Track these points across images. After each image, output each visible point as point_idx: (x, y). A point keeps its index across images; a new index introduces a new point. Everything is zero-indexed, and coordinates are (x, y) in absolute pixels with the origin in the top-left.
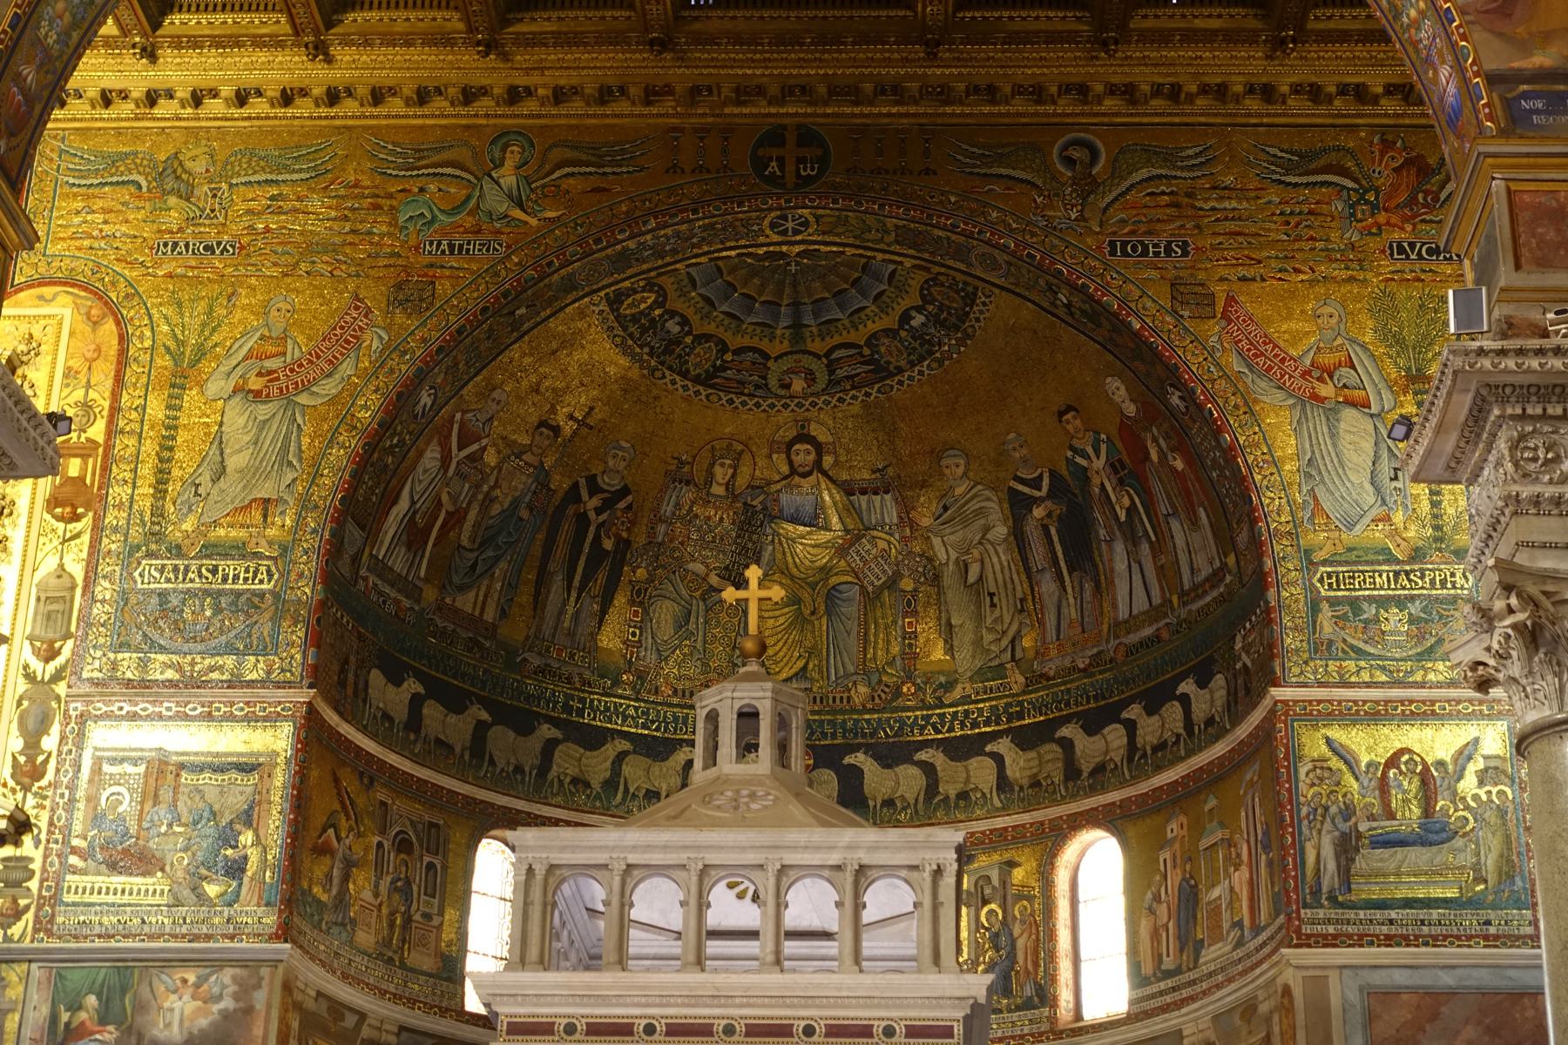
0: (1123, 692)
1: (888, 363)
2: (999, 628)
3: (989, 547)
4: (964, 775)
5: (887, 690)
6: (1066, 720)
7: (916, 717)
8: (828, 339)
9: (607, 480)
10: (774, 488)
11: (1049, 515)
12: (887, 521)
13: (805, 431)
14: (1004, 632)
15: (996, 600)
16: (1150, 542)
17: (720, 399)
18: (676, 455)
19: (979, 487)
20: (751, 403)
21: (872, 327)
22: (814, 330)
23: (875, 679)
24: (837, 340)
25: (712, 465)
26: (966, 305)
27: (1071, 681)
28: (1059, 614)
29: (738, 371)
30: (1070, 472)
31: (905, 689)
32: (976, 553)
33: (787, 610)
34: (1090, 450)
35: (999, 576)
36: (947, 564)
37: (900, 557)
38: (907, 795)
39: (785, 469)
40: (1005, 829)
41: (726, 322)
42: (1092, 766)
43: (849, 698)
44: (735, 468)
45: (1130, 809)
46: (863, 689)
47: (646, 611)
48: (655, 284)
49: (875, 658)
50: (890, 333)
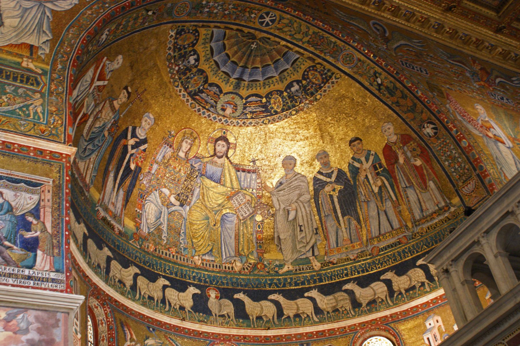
0: (379, 268)
1: (272, 108)
2: (304, 241)
3: (301, 204)
4: (296, 306)
5: (250, 266)
7: (266, 280)
8: (250, 90)
9: (140, 132)
10: (206, 160)
11: (334, 190)
12: (252, 187)
13: (225, 135)
14: (307, 243)
15: (303, 228)
17: (195, 108)
18: (169, 130)
19: (299, 176)
20: (207, 114)
21: (272, 88)
22: (246, 83)
23: (244, 260)
24: (254, 91)
25: (182, 141)
26: (323, 82)
27: (347, 265)
28: (337, 235)
29: (208, 95)
30: (349, 170)
31: (259, 266)
33: (203, 222)
34: (363, 159)
35: (305, 218)
36: (279, 210)
38: (268, 315)
39: (212, 153)
40: (324, 331)
41: (213, 67)
42: (367, 301)
43: (232, 268)
44: (191, 145)
45: (398, 318)
46: (239, 264)
47: (144, 205)
48: (197, 31)
49: (243, 250)
50: (280, 93)
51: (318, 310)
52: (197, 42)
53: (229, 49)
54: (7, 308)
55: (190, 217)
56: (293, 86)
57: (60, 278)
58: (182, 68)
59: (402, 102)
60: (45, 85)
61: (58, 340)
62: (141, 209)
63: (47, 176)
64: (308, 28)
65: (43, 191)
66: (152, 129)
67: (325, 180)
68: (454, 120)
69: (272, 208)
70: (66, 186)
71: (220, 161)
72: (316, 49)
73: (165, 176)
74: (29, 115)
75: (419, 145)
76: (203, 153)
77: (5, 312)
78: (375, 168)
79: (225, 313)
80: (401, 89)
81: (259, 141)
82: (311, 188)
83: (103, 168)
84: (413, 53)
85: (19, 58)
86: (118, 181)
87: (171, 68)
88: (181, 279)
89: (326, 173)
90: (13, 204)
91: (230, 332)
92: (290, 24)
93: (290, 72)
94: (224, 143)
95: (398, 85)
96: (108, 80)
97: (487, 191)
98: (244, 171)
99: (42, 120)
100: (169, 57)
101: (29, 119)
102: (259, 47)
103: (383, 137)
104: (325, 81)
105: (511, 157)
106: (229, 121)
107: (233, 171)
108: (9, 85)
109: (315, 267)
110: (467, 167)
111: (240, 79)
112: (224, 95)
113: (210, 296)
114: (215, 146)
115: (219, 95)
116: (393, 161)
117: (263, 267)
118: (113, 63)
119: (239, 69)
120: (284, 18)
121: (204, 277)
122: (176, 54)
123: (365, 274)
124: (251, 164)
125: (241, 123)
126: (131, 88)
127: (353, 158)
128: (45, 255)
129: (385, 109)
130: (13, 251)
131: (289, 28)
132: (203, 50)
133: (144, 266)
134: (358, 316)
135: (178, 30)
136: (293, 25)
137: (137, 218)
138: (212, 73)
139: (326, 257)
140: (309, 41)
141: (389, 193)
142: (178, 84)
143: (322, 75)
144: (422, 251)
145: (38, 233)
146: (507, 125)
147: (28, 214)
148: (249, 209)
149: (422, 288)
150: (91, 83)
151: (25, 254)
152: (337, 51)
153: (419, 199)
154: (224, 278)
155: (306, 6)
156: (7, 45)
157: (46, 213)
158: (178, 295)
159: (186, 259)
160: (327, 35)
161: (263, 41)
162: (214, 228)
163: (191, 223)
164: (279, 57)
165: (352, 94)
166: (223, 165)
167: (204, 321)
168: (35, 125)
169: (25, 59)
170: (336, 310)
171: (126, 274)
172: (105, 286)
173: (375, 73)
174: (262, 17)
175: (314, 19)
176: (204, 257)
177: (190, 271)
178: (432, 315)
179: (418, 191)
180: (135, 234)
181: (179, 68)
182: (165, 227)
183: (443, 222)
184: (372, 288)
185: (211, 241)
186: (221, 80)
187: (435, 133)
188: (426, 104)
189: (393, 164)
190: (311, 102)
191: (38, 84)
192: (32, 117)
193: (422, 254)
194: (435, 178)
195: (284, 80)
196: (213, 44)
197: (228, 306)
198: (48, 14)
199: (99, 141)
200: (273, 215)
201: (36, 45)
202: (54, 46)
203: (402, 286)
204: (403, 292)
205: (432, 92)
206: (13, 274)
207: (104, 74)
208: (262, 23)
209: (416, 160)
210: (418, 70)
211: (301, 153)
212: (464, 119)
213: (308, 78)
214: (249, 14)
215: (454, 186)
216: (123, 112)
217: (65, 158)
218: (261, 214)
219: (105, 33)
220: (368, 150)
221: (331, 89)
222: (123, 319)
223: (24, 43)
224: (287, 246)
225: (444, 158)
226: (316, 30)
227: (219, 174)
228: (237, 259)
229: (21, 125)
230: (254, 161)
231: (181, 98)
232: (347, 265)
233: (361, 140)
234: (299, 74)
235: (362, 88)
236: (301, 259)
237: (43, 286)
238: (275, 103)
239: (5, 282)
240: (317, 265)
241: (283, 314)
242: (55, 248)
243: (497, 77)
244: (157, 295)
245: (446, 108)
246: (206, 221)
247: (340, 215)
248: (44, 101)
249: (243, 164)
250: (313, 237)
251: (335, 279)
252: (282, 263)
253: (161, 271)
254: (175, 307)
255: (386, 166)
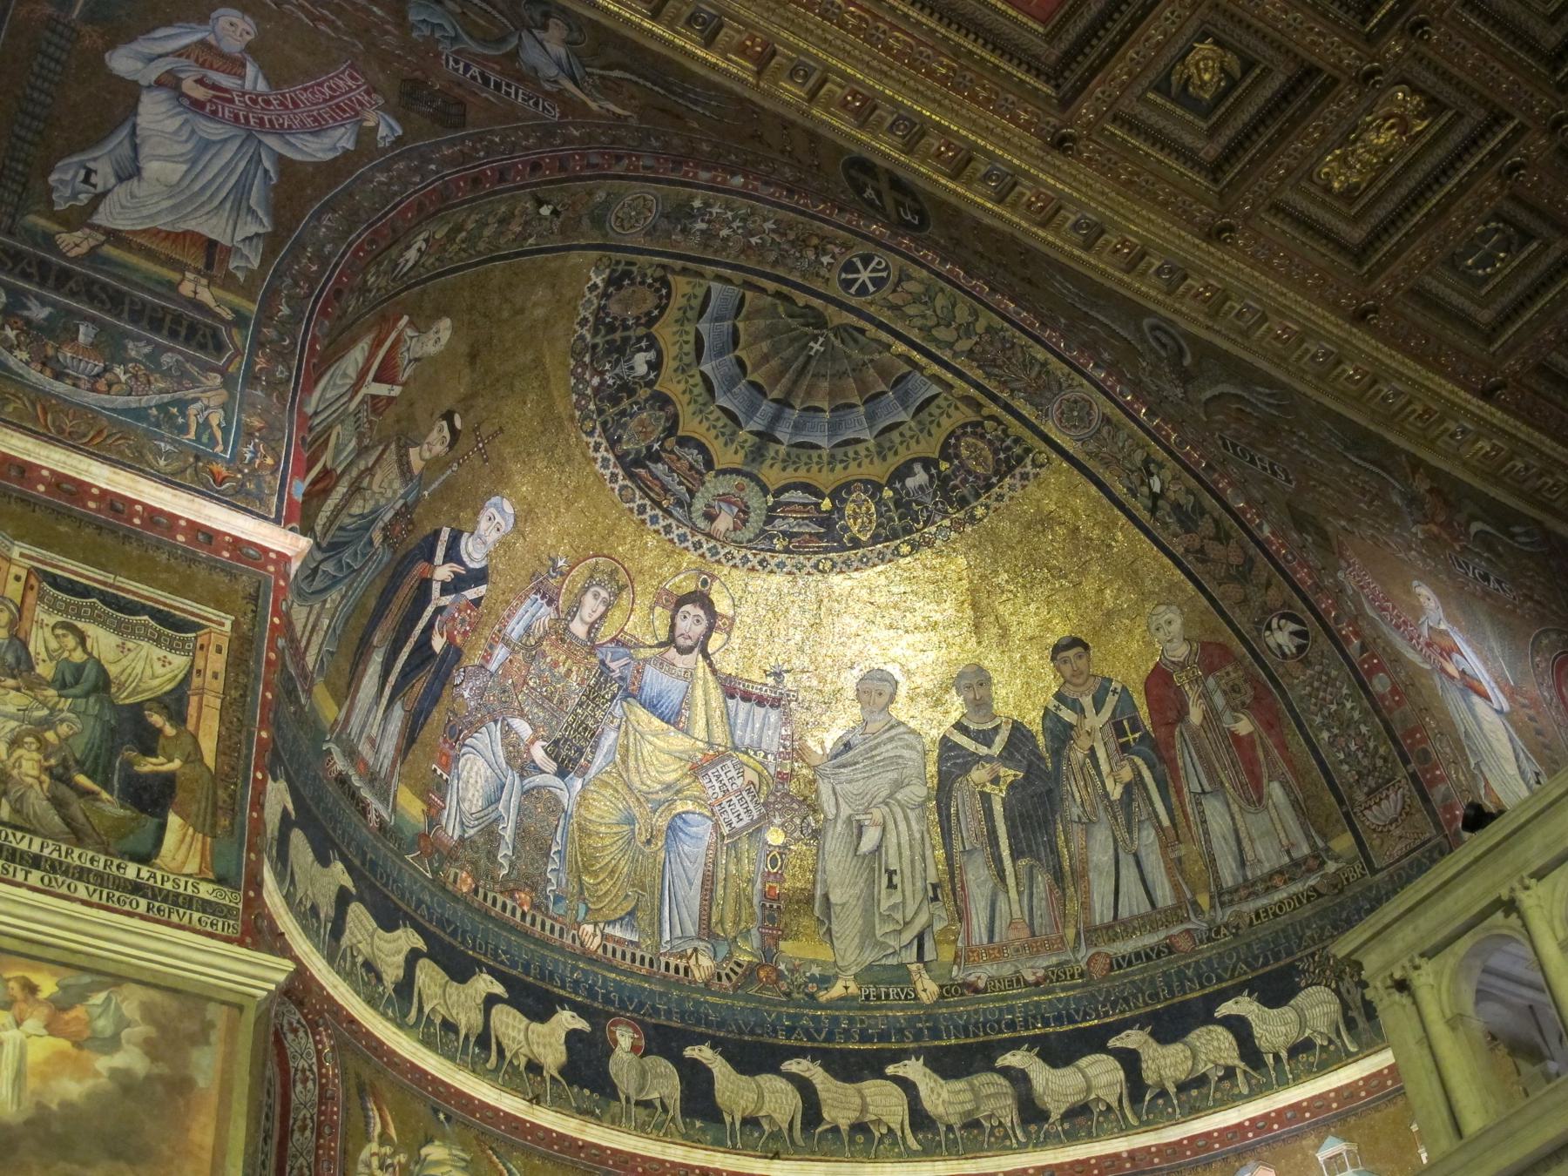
0: (1106, 1014)
1: (846, 529)
2: (899, 916)
3: (897, 810)
4: (858, 1101)
5: (737, 969)
6: (1014, 1045)
7: (779, 1016)
8: (790, 470)
9: (470, 548)
11: (995, 781)
12: (764, 746)
15: (896, 879)
16: (1159, 827)
17: (633, 500)
18: (553, 554)
19: (902, 729)
20: (662, 523)
21: (854, 472)
22: (783, 449)
23: (723, 951)
24: (801, 475)
25: (585, 590)
26: (996, 473)
31: (762, 974)
32: (877, 814)
34: (1087, 701)
35: (906, 853)
37: (772, 799)
38: (775, 1116)
39: (663, 635)
41: (696, 391)
43: (686, 970)
44: (609, 606)
45: (1152, 1163)
46: (705, 962)
47: (457, 759)
48: (665, 283)
49: (721, 921)
51: (920, 1119)
52: (662, 313)
53: (749, 345)
54: (62, 970)
55: (582, 811)
56: (911, 473)
57: (226, 902)
58: (610, 382)
59: (1214, 550)
60: (238, 352)
61: (202, 1083)
62: (446, 767)
63: (219, 606)
64: (975, 314)
65: (202, 647)
66: (505, 544)
67: (972, 749)
68: (1356, 618)
69: (815, 811)
70: (272, 640)
71: (684, 662)
72: (988, 375)
73: (525, 683)
74: (184, 429)
75: (1252, 679)
76: (638, 633)
77: (55, 980)
78: (1119, 730)
79: (655, 1095)
80: (1216, 515)
81: (798, 617)
82: (932, 769)
83: (355, 637)
84: (1254, 423)
85: (174, 270)
86: (392, 679)
87: (580, 379)
88: (539, 983)
89: (979, 731)
90: (113, 670)
91: (663, 1153)
92: (928, 297)
93: (908, 434)
94: (701, 613)
95: (1209, 501)
96: (404, 384)
97: (1438, 825)
98: (746, 697)
99: (219, 449)
100: (580, 345)
101: (184, 439)
102: (829, 354)
103: (1149, 644)
104: (1004, 468)
105: (1505, 739)
106: (723, 552)
107: (716, 695)
108: (138, 338)
109: (923, 996)
110: (1382, 751)
111: (766, 437)
112: (716, 476)
113: (616, 1042)
114: (673, 618)
115: (702, 474)
116: (1172, 715)
117: (774, 977)
118: (423, 338)
119: (767, 408)
120: (909, 278)
121: (604, 986)
122: (598, 340)
123: (1065, 1028)
124: (770, 681)
125: (755, 562)
126: (462, 418)
127: (1059, 696)
128: (191, 830)
129: (1163, 566)
130: (99, 804)
131: (923, 308)
132: (677, 338)
133: (438, 931)
134: (1035, 1146)
135: (614, 271)
136: (932, 299)
137: (433, 791)
138: (692, 408)
139: (955, 968)
140: (971, 351)
141: (1152, 804)
142: (594, 428)
143: (996, 452)
144: (1232, 977)
145: (176, 764)
146: (1497, 651)
147: (155, 705)
148: (751, 807)
149: (1227, 1084)
150: (354, 386)
151: (133, 819)
152: (1048, 387)
153: (1236, 831)
154: (661, 994)
155: (976, 252)
156: (144, 231)
157: (205, 710)
158: (527, 1029)
159: (557, 928)
160: (1024, 340)
161: (845, 335)
162: (647, 850)
163: (581, 829)
164: (883, 388)
165: (1075, 512)
166: (689, 675)
167: (592, 1114)
168: (197, 458)
169: (189, 275)
170: (972, 1124)
171: (386, 947)
172: (324, 971)
173: (1147, 461)
174: (850, 267)
175: (993, 290)
176: (608, 930)
177: (565, 964)
178: (1251, 1163)
179: (1235, 808)
180: (425, 836)
181: (603, 382)
182: (508, 831)
183: (1300, 902)
184: (1080, 1070)
185: (633, 886)
186: (713, 432)
187: (1301, 649)
188: (1282, 563)
189: (1173, 725)
190: (957, 526)
191: (220, 348)
192: (192, 435)
193: (1233, 987)
194: (1289, 776)
195: (890, 455)
196: (704, 326)
197: (664, 1076)
198: (267, 164)
199: (356, 554)
200: (816, 834)
201: (225, 241)
202: (274, 253)
203: (1168, 1073)
204: (1172, 1090)
205: (1300, 532)
206: (90, 871)
207: (395, 367)
208: (847, 284)
209: (1237, 720)
210: (1264, 469)
211: (912, 666)
212: (1383, 618)
213: (957, 456)
214: (817, 255)
215: (1341, 802)
216: (430, 484)
217: (275, 562)
218: (782, 825)
219: (416, 246)
220: (1104, 678)
221: (1019, 493)
222: (367, 1074)
223: (193, 233)
224: (847, 926)
225: (1318, 719)
226: (997, 322)
227: (676, 697)
228: (701, 945)
229: (158, 453)
230: (778, 675)
231: (597, 467)
232: (1014, 997)
233: (1086, 647)
234: (932, 441)
235: (1105, 501)
236: (884, 966)
237: (174, 918)
238: (855, 517)
239: (64, 890)
240: (927, 988)
241: (819, 1119)
242: (220, 812)
243: (1473, 518)
244: (468, 1019)
245: (1336, 580)
246: (627, 828)
247: (1006, 853)
248: (232, 396)
249: (746, 676)
250: (925, 908)
251: (976, 1035)
252: (831, 972)
253: (485, 955)
254: (516, 1062)
255: (1149, 727)
